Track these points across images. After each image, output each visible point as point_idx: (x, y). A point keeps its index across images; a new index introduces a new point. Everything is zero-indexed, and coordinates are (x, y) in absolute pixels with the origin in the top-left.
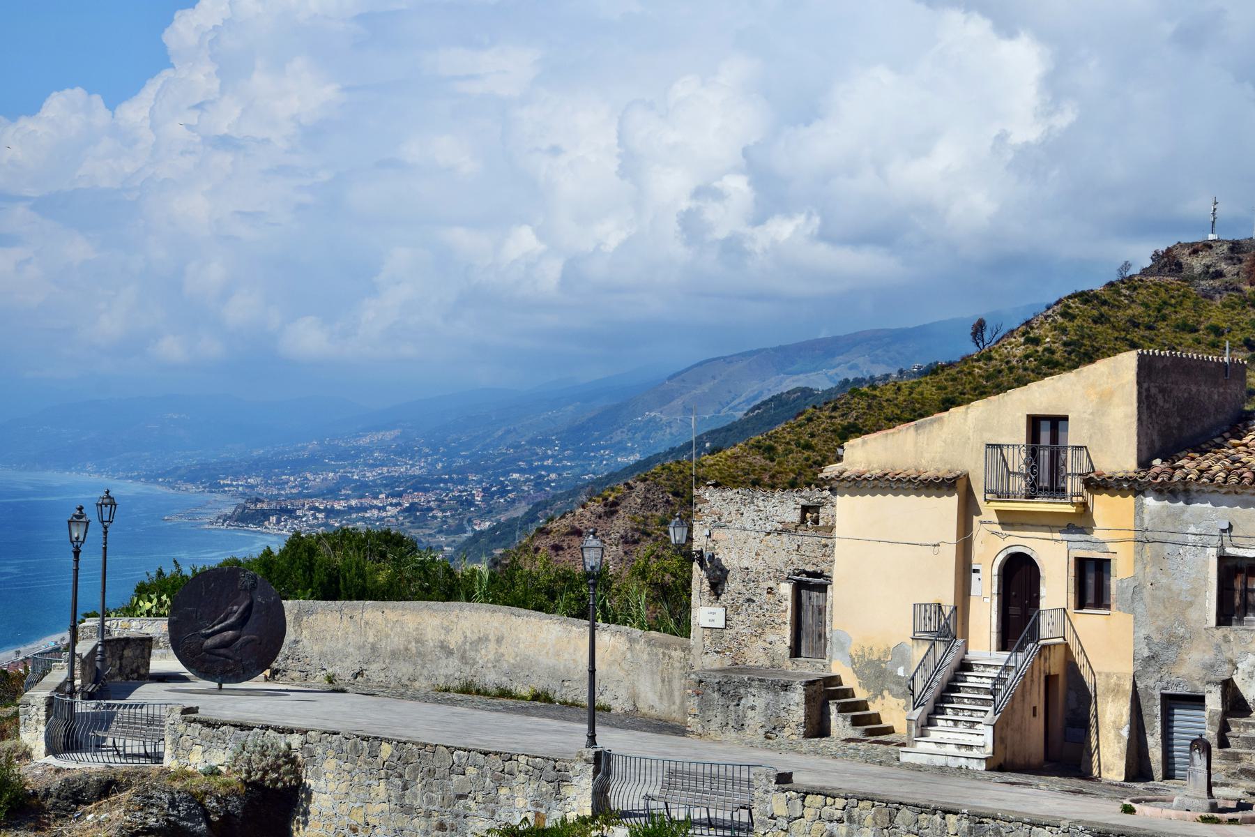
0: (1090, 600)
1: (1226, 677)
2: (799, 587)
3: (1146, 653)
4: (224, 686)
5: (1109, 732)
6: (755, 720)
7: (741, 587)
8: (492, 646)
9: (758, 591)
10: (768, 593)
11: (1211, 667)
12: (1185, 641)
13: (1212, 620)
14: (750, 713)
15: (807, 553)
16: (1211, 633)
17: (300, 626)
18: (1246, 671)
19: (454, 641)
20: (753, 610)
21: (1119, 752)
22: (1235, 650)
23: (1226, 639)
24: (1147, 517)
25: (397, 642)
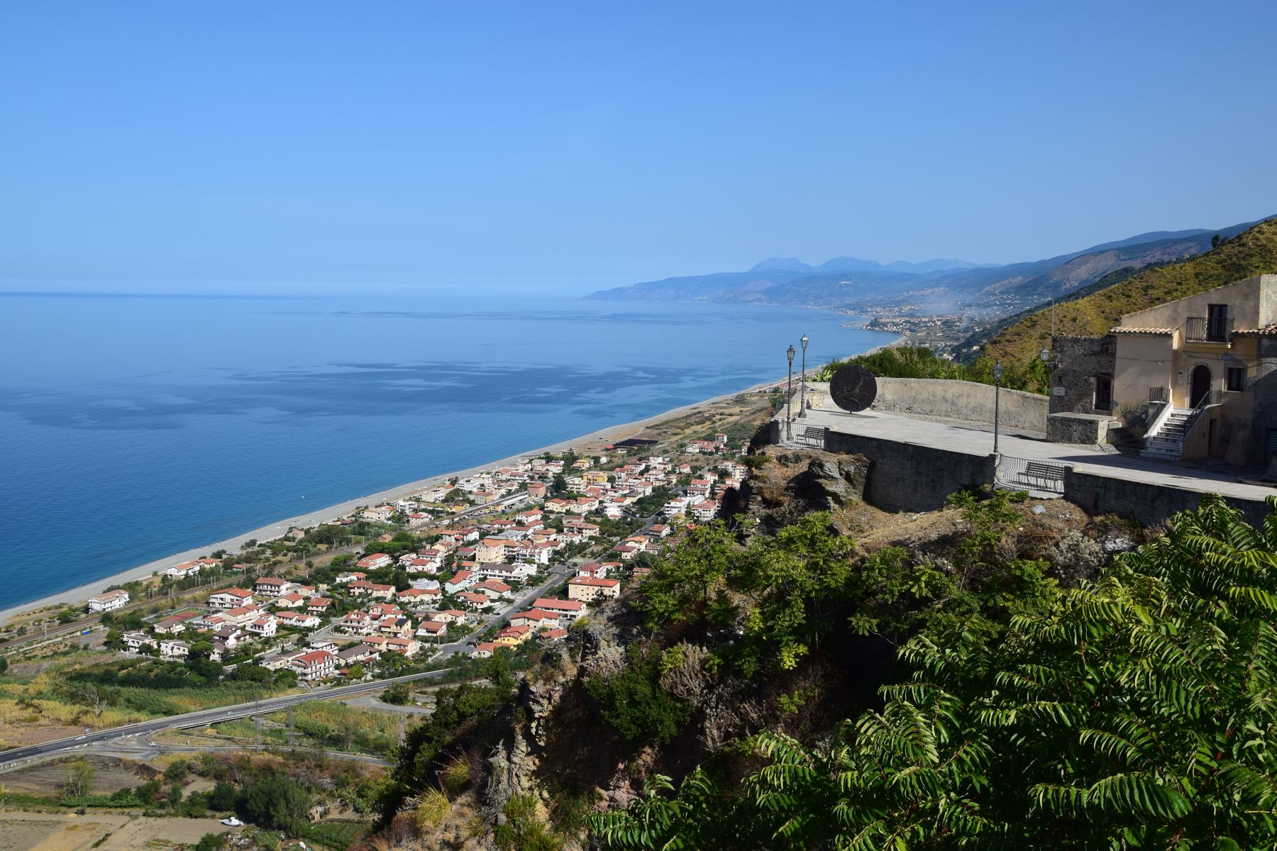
3: (1259, 410)
8: (965, 399)
14: (1075, 433)
19: (949, 396)
24: (1263, 350)
25: (925, 396)
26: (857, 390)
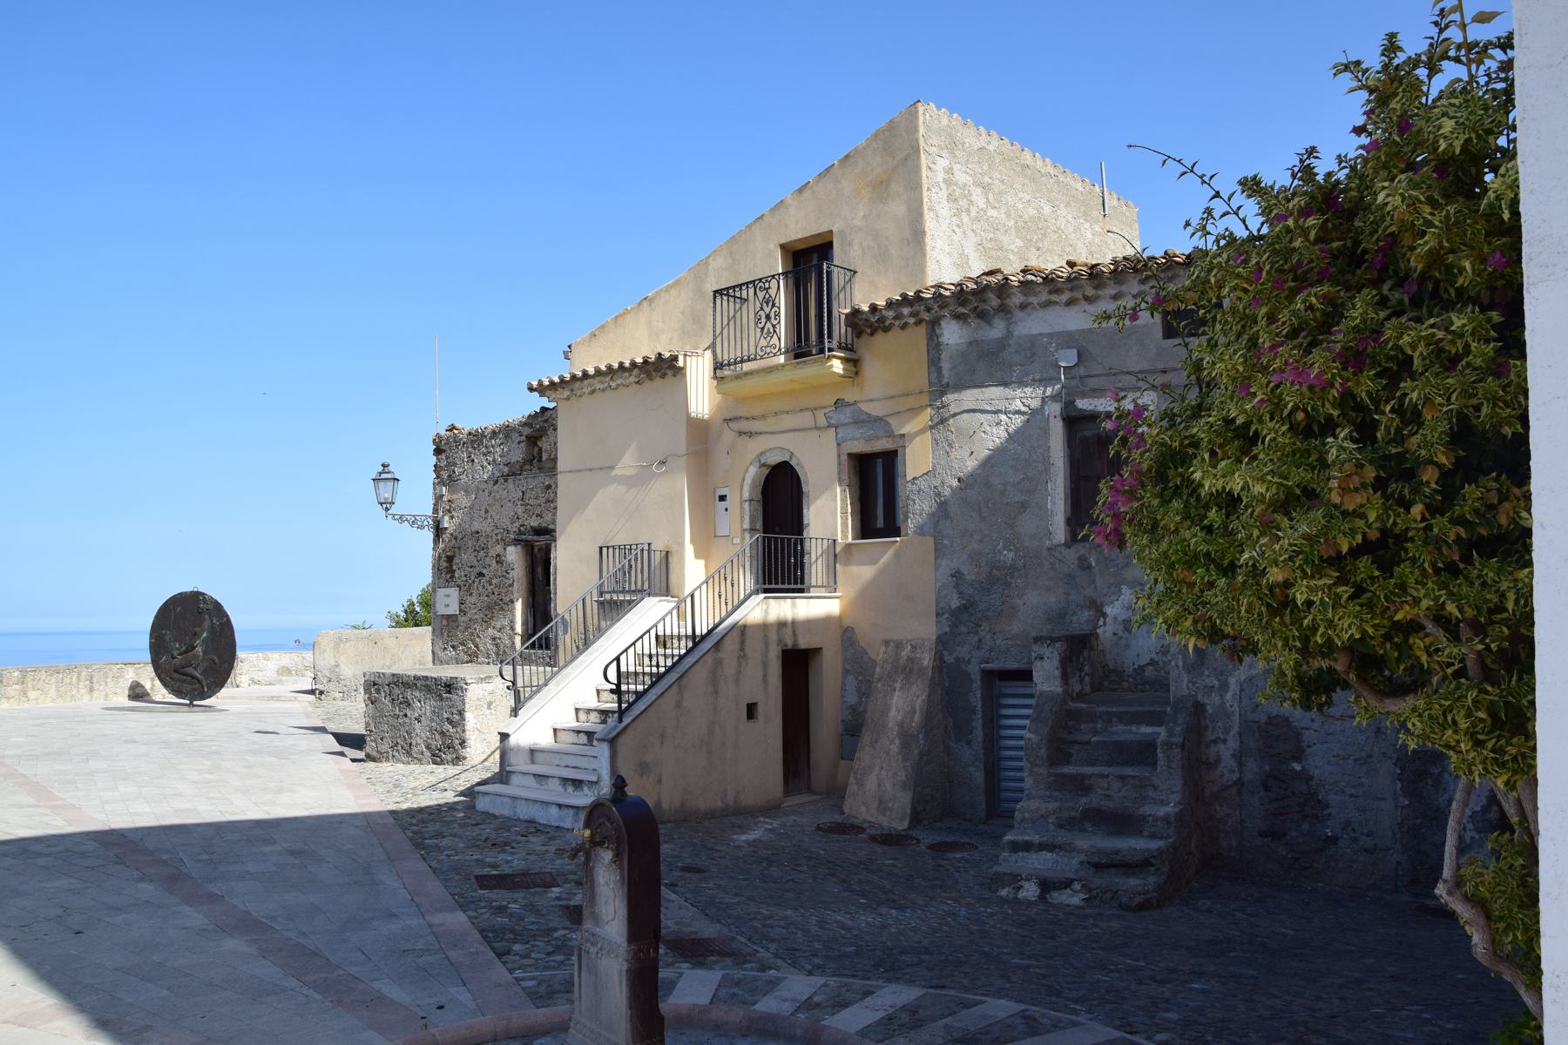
0: (880, 523)
1: (1086, 629)
2: (529, 548)
3: (955, 603)
4: (195, 703)
5: (892, 742)
6: (421, 733)
7: (472, 558)
9: (488, 561)
10: (497, 562)
11: (1061, 615)
12: (1016, 574)
13: (1060, 533)
15: (531, 502)
16: (1058, 554)
17: (338, 652)
18: (1120, 619)
20: (484, 587)
21: (904, 778)
22: (1099, 582)
23: (1084, 564)
24: (946, 365)
26: (199, 650)
